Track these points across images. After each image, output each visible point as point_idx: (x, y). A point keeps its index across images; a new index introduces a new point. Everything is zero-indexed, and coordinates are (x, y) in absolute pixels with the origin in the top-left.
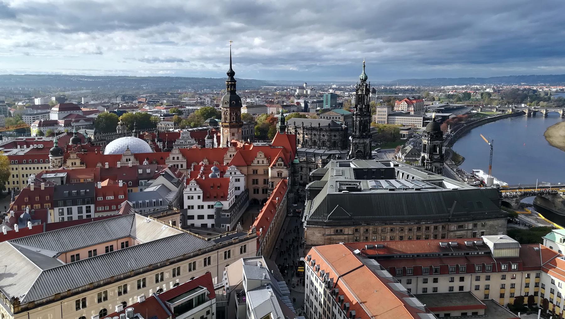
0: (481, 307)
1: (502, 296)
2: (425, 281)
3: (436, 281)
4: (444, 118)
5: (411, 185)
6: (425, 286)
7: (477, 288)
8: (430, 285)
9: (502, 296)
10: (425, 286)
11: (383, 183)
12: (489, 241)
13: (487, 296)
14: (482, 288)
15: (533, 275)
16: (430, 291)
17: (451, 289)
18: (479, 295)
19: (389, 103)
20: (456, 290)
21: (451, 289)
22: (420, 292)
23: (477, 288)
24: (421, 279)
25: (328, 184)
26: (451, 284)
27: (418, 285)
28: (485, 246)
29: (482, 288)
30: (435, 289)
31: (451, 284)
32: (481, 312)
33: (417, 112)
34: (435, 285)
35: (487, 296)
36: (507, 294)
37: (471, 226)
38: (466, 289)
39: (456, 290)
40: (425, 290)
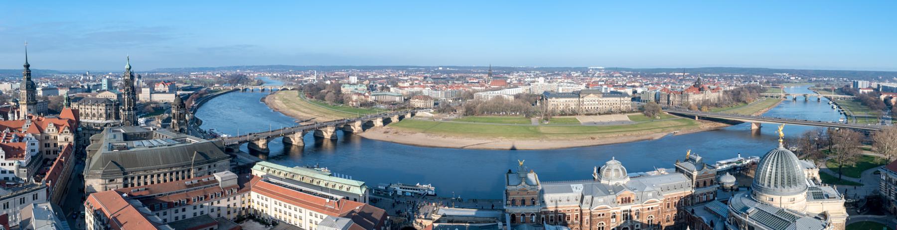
0: (215, 223)
1: (229, 213)
2: (177, 212)
3: (184, 210)
4: (189, 95)
5: (164, 143)
6: (177, 215)
7: (212, 211)
8: (180, 214)
9: (229, 213)
10: (177, 215)
11: (145, 142)
12: (218, 176)
13: (219, 215)
14: (215, 210)
15: (246, 195)
16: (180, 219)
17: (195, 214)
18: (214, 215)
19: (151, 85)
20: (198, 214)
21: (195, 214)
22: (173, 220)
23: (212, 211)
24: (173, 210)
25: (104, 145)
26: (195, 211)
27: (171, 215)
28: (215, 181)
29: (215, 210)
30: (184, 217)
31: (195, 211)
32: (216, 227)
33: (171, 91)
34: (184, 213)
35: (219, 215)
36: (232, 211)
37: (207, 168)
38: (205, 213)
39: (198, 214)
40: (177, 218)
